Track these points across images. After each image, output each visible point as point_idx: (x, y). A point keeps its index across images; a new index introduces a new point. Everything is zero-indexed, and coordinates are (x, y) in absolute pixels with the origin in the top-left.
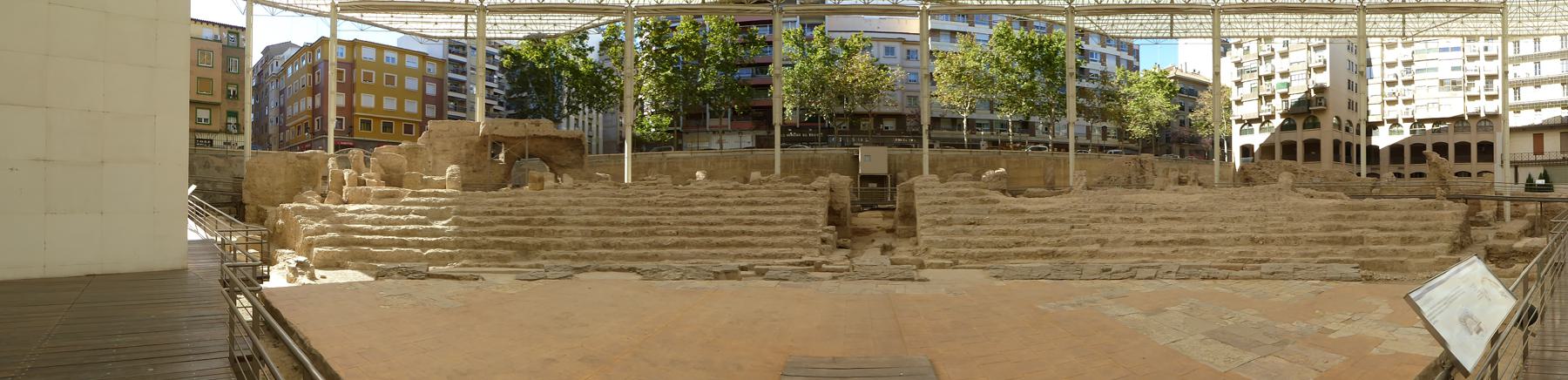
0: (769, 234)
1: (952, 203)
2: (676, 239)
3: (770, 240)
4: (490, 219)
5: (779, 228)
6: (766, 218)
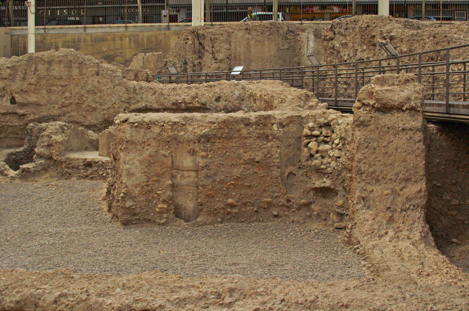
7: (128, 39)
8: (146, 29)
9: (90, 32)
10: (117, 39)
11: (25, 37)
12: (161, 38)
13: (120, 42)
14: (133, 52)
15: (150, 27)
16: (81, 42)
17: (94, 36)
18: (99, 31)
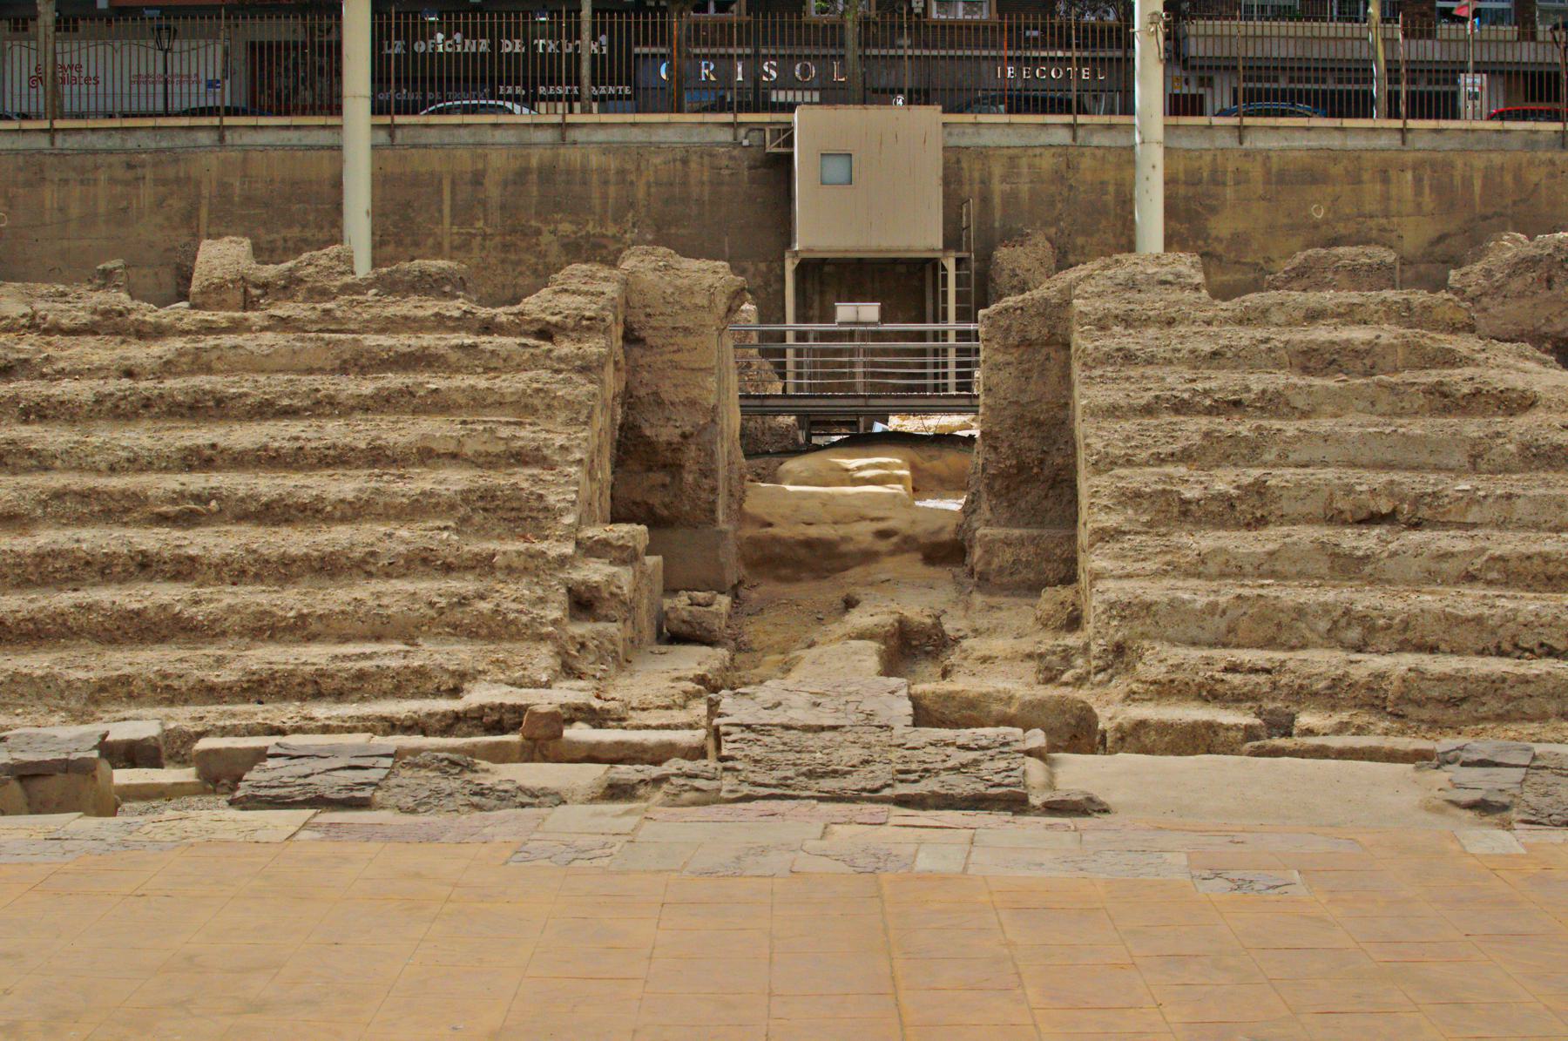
0: (284, 570)
1: (1272, 403)
3: (290, 600)
5: (339, 536)
6: (266, 485)
7: (1409, 176)
8: (1478, 142)
9: (1260, 145)
10: (1366, 176)
11: (1127, 157)
12: (1535, 179)
13: (1378, 187)
14: (1431, 230)
15: (1495, 136)
16: (1224, 184)
17: (1275, 159)
18: (1296, 144)
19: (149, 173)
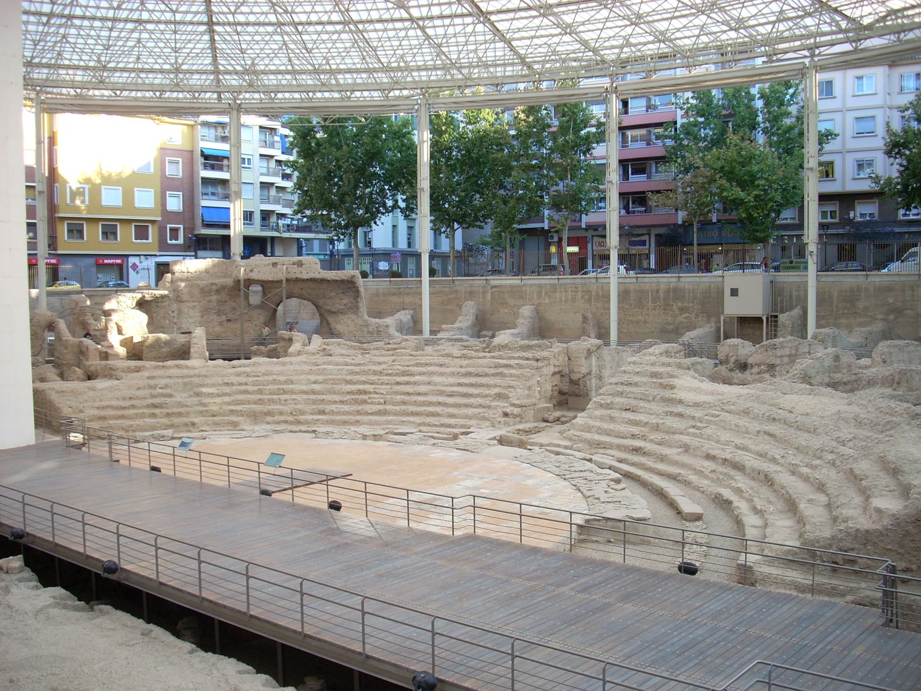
2: (381, 407)
4: (227, 390)
13: (910, 292)
19: (580, 289)
